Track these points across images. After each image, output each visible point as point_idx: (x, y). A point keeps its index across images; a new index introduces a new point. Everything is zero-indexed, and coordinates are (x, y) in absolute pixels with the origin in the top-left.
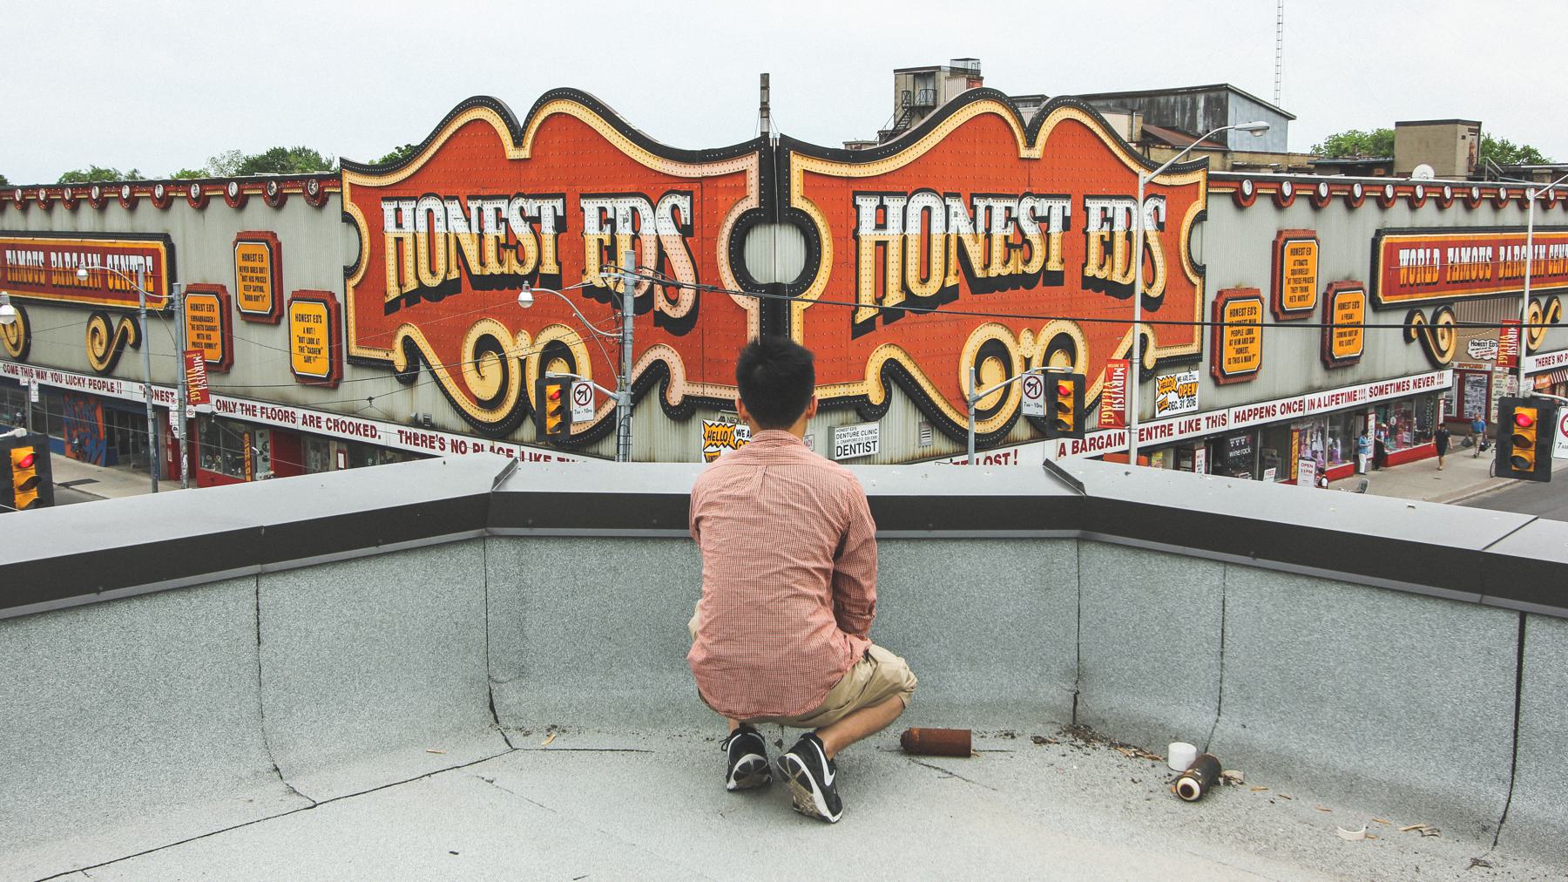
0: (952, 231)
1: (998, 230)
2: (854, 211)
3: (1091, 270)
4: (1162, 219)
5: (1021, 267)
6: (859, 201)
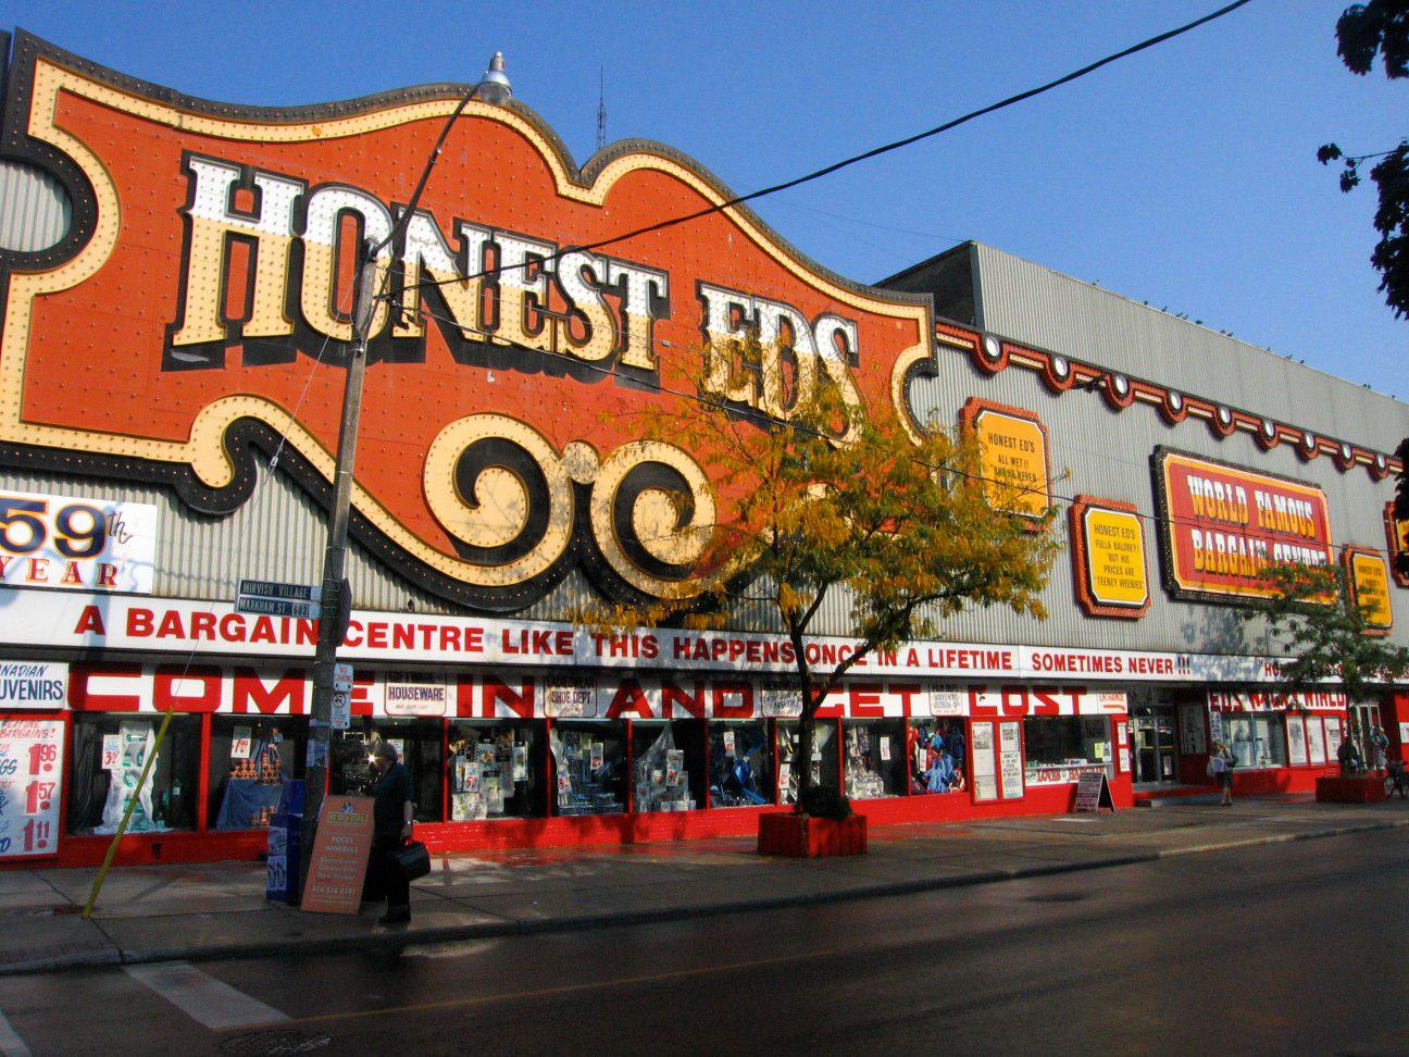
0: (410, 260)
1: (512, 283)
2: (183, 180)
3: (717, 382)
4: (852, 349)
5: (563, 345)
6: (196, 166)
